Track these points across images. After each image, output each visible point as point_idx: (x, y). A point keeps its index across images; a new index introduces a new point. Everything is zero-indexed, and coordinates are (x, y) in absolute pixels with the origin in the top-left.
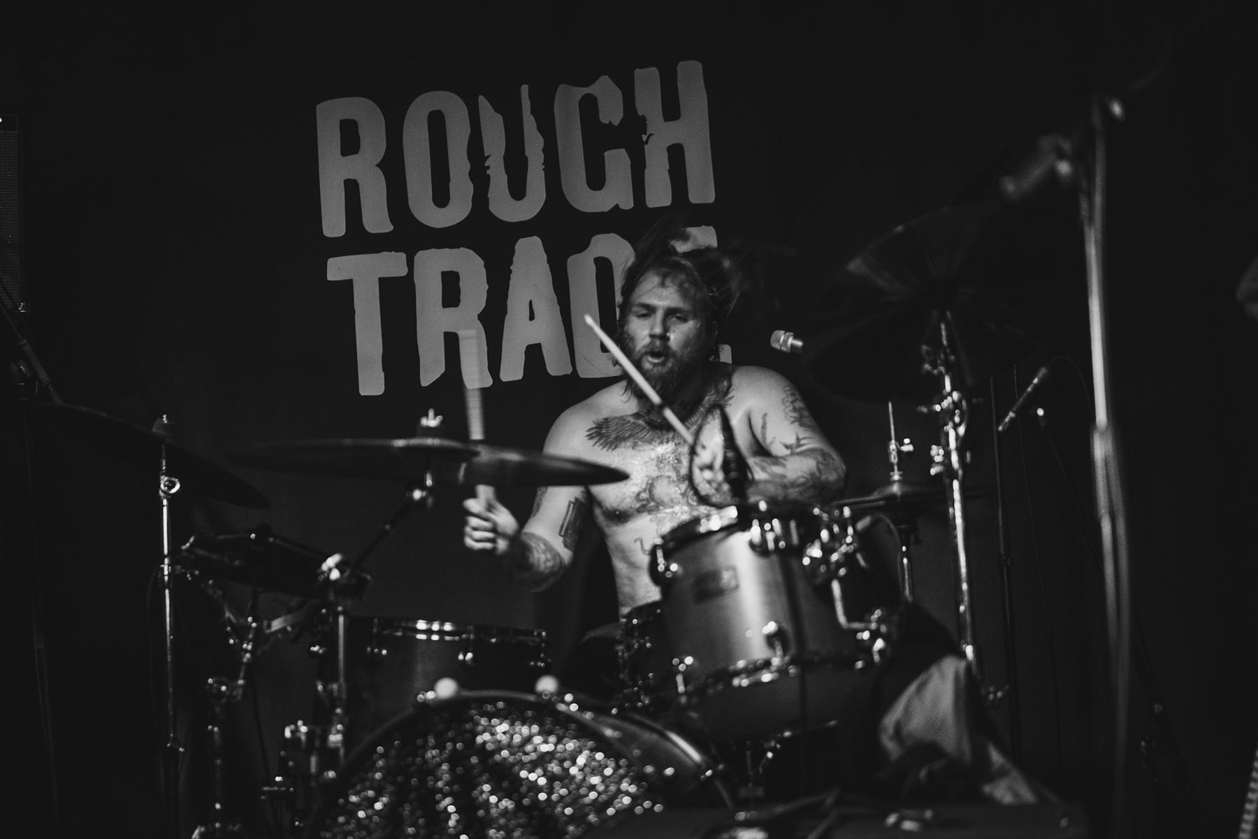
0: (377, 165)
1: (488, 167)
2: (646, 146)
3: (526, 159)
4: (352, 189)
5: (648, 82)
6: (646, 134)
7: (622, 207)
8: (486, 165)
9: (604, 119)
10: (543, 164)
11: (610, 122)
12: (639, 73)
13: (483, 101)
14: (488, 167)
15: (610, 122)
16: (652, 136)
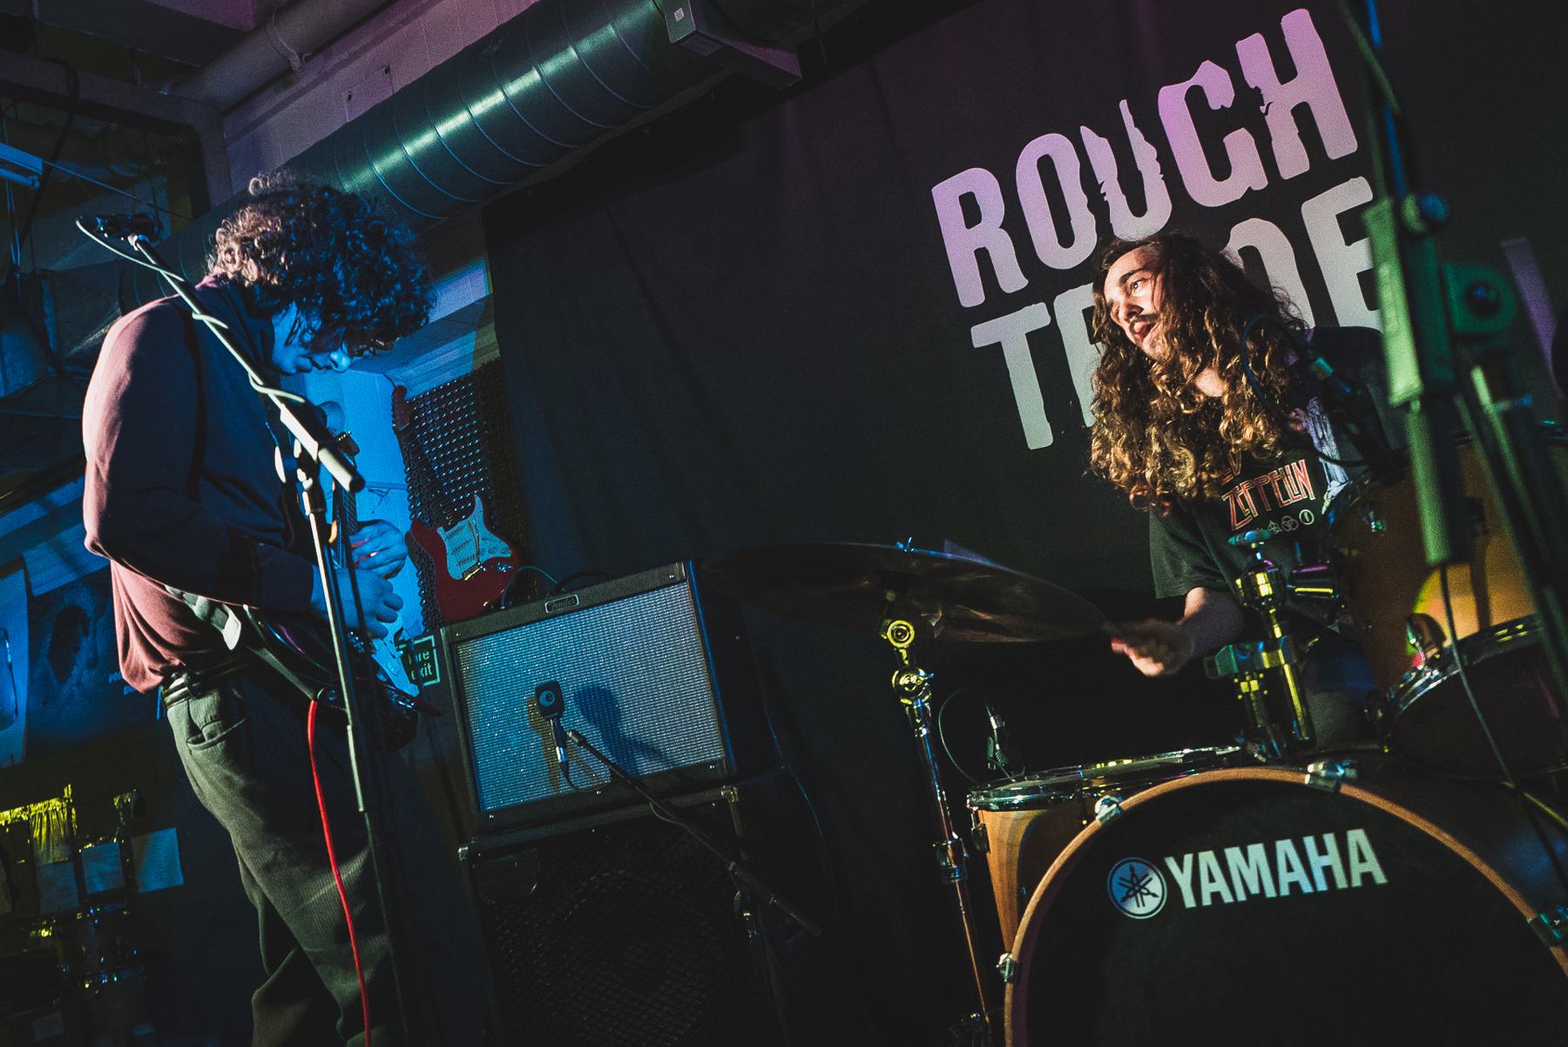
0: (1001, 227)
1: (1104, 194)
2: (1267, 118)
3: (1140, 173)
4: (983, 256)
5: (1253, 51)
6: (1263, 105)
7: (1255, 188)
8: (1102, 192)
9: (1215, 105)
10: (1161, 173)
11: (1222, 106)
12: (1241, 46)
13: (1086, 133)
14: (1104, 194)
15: (1222, 106)
16: (1271, 106)
